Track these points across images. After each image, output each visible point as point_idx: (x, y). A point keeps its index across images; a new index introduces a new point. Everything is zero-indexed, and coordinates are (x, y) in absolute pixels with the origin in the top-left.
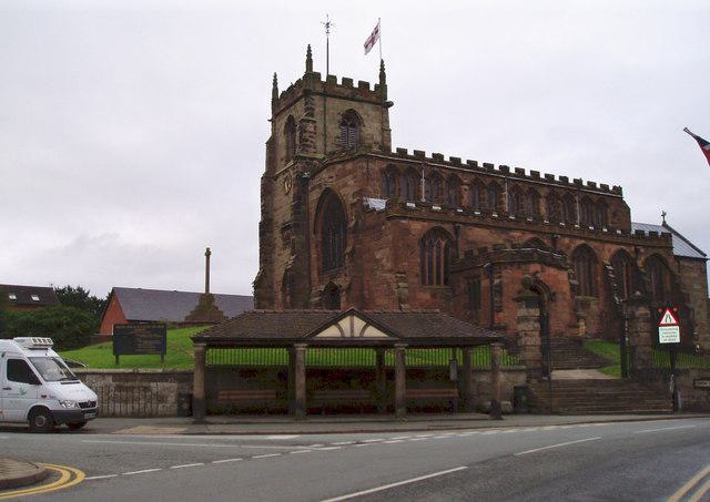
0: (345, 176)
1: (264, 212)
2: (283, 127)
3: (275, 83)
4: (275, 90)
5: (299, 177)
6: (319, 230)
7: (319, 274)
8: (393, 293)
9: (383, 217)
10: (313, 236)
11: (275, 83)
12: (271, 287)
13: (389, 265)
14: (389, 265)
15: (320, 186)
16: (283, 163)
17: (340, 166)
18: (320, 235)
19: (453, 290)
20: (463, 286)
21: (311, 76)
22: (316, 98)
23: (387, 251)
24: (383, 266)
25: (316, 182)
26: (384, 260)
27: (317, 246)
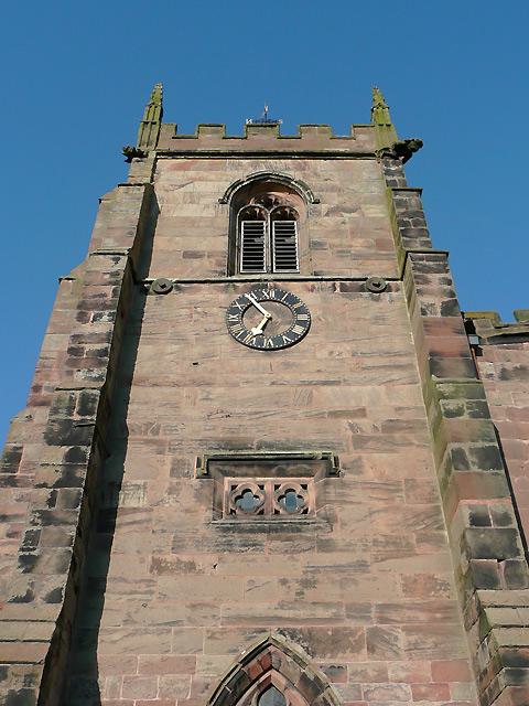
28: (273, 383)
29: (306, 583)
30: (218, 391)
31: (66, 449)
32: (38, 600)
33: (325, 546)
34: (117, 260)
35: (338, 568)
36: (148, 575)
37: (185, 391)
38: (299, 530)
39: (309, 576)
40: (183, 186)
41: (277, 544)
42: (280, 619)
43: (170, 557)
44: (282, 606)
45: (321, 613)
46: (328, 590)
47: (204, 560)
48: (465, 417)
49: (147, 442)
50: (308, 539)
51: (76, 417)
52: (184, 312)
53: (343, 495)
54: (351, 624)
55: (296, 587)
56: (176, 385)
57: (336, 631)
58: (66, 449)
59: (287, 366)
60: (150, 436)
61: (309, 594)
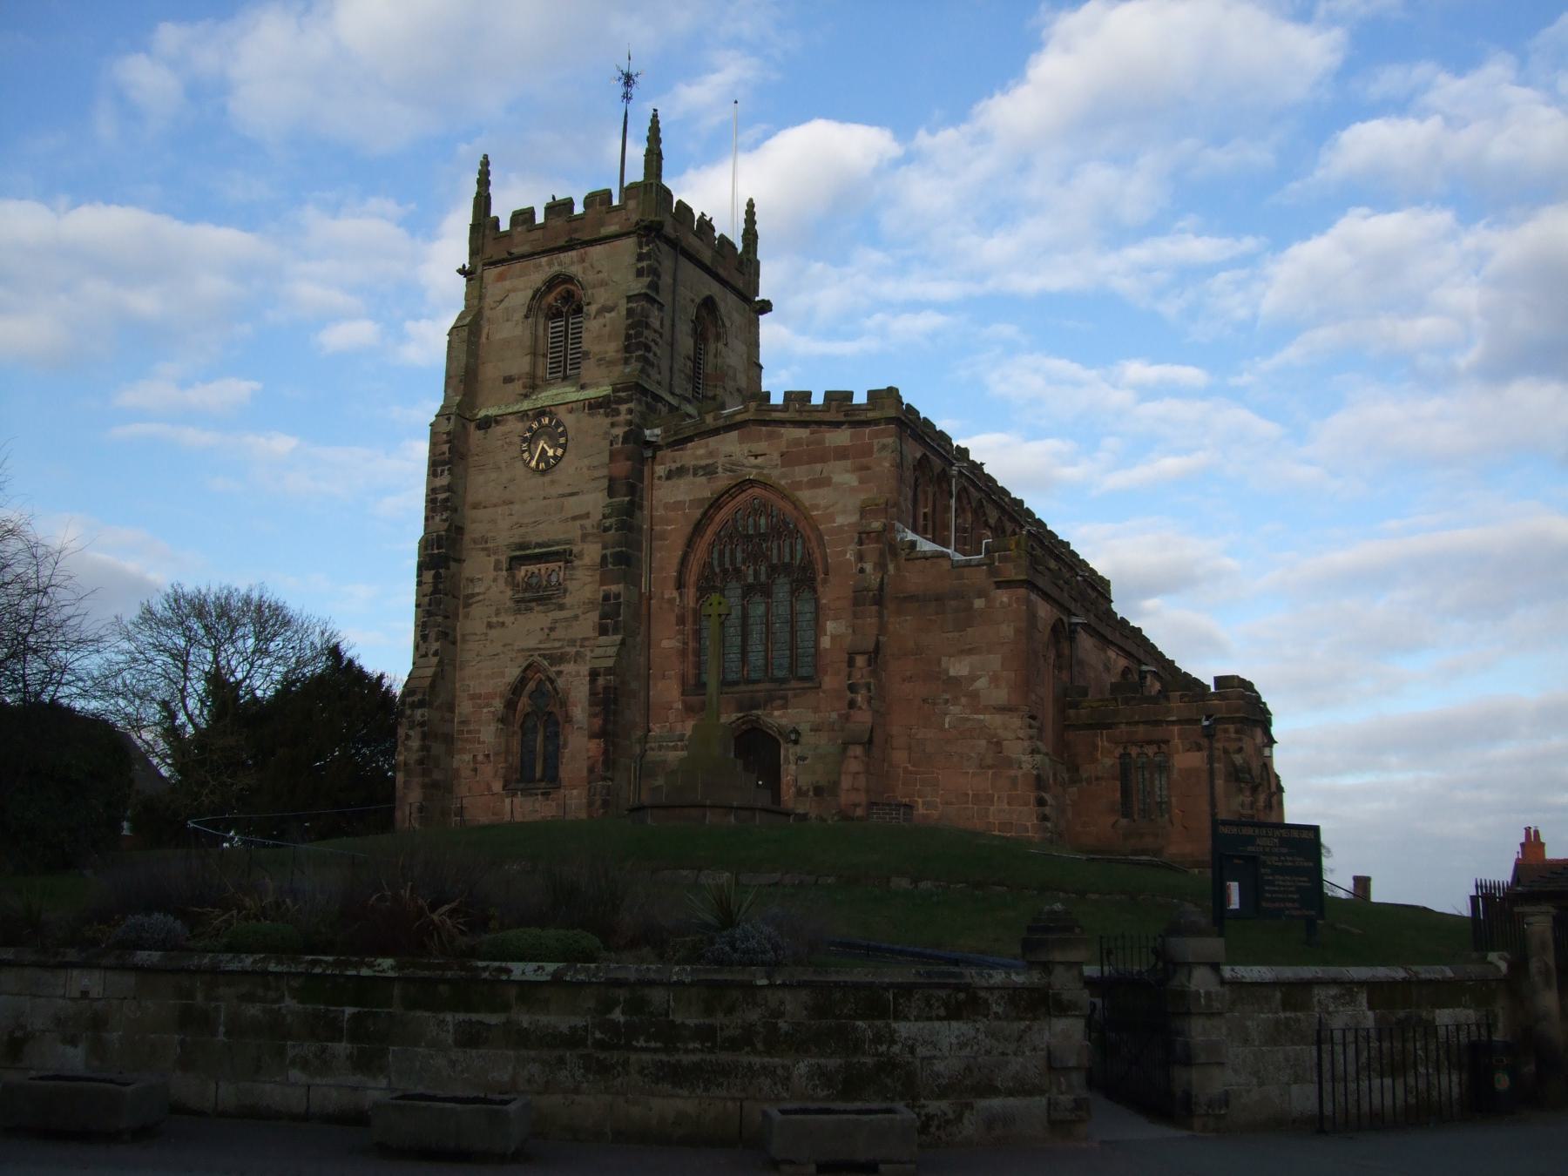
0: (823, 458)
1: (433, 505)
2: (521, 298)
3: (484, 181)
4: (482, 202)
5: (634, 436)
6: (692, 578)
7: (683, 693)
8: (1009, 763)
9: (980, 577)
10: (671, 593)
11: (484, 181)
12: (451, 707)
13: (1001, 695)
14: (1001, 695)
15: (709, 471)
16: (517, 387)
17: (803, 433)
18: (691, 592)
19: (1074, 769)
20: (1108, 762)
21: (652, 189)
22: (665, 248)
23: (995, 661)
24: (974, 695)
25: (696, 453)
26: (981, 683)
27: (681, 620)
28: (545, 498)
29: (552, 629)
30: (516, 507)
31: (433, 572)
32: (430, 656)
33: (561, 607)
34: (449, 419)
35: (566, 619)
36: (485, 631)
37: (499, 510)
38: (550, 599)
39: (553, 626)
40: (502, 301)
41: (541, 607)
42: (539, 649)
43: (494, 620)
44: (540, 642)
45: (557, 644)
46: (560, 633)
47: (508, 619)
48: (613, 531)
49: (483, 549)
50: (555, 604)
51: (436, 551)
52: (500, 443)
53: (572, 575)
54: (568, 649)
55: (546, 631)
56: (495, 506)
57: (562, 653)
58: (433, 572)
59: (553, 482)
60: (484, 546)
61: (553, 635)
